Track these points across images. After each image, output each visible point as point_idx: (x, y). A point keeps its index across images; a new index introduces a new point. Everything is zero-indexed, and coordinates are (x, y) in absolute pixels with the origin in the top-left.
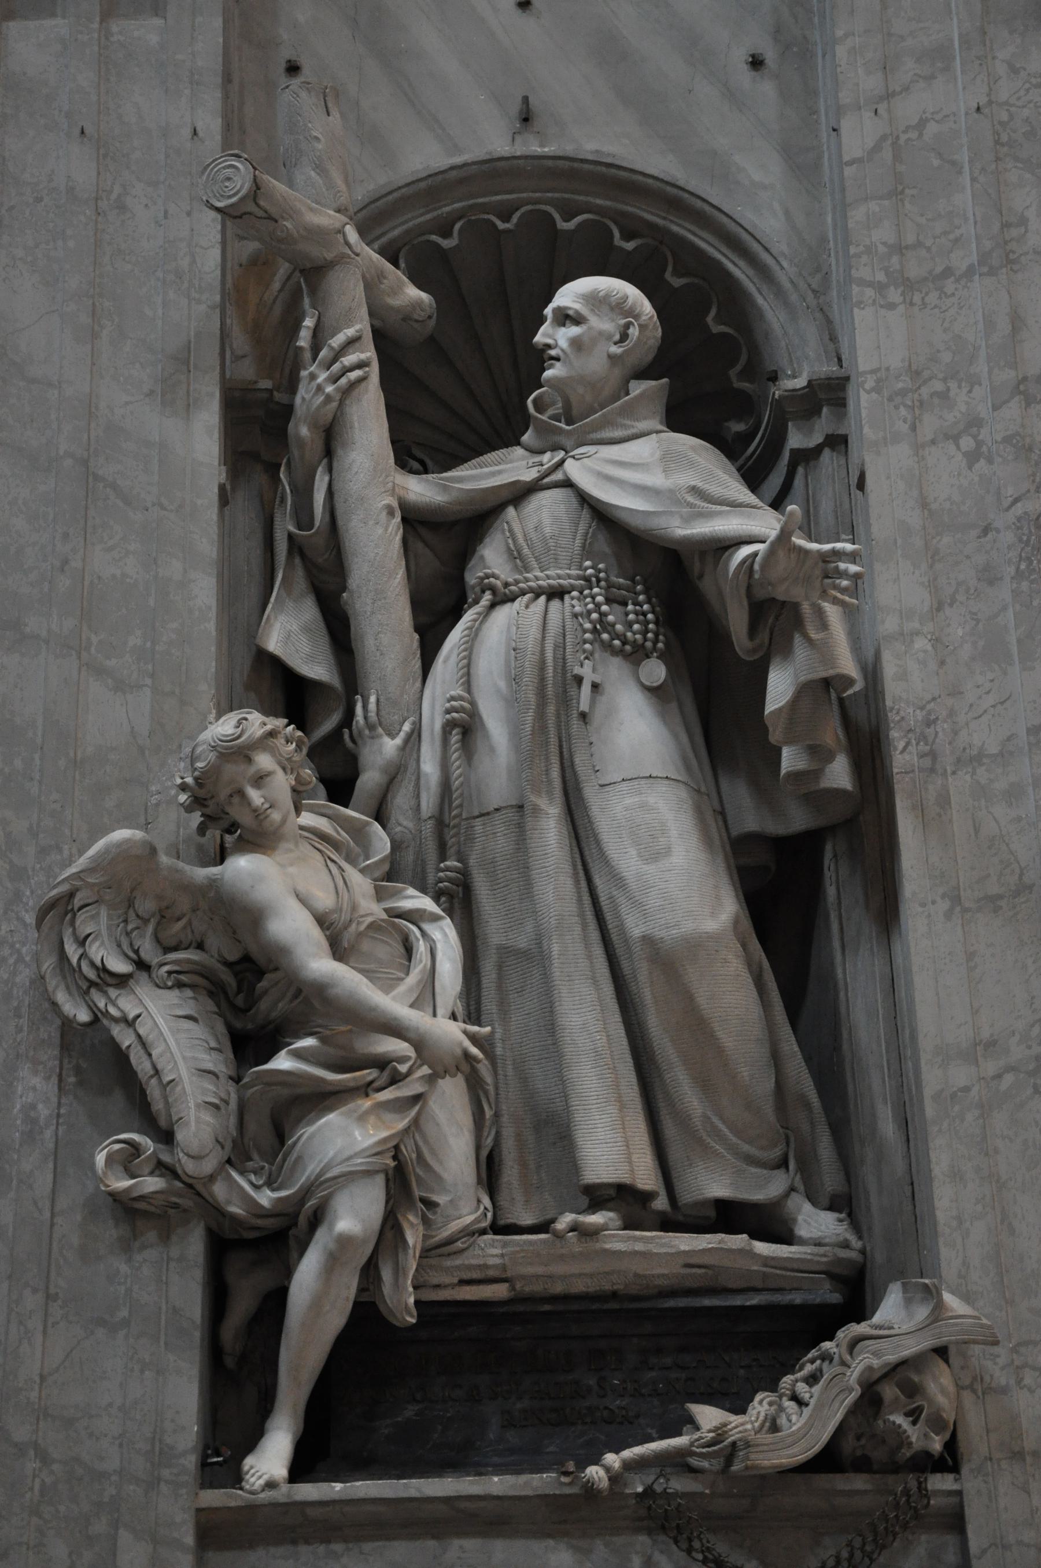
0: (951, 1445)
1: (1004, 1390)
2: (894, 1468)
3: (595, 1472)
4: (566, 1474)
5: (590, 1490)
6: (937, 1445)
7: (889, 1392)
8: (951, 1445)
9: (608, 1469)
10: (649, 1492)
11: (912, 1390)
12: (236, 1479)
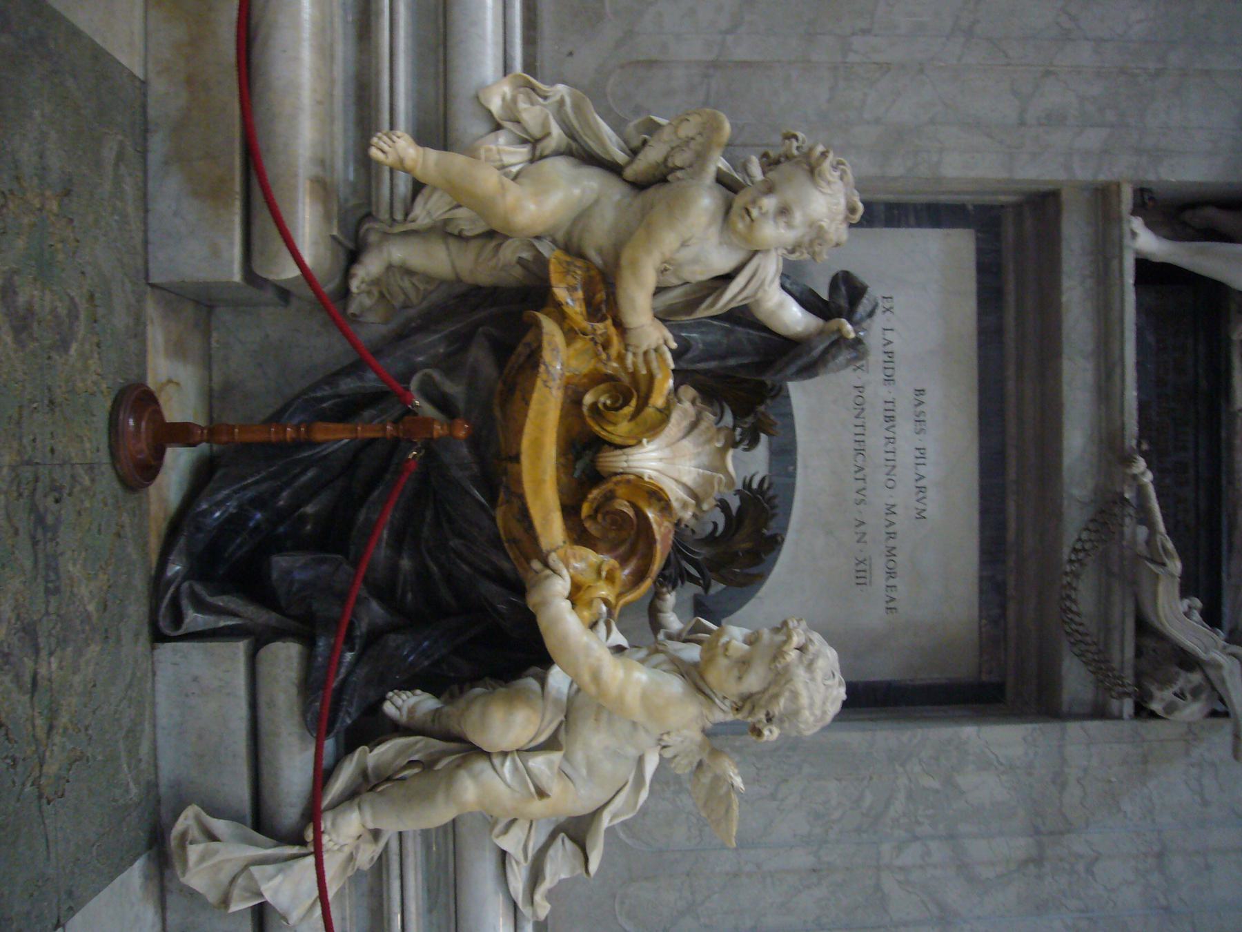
0: (1153, 715)
1: (1187, 753)
2: (1139, 675)
3: (1141, 464)
4: (1139, 444)
5: (1128, 461)
6: (1156, 706)
7: (1196, 678)
8: (1153, 715)
9: (1143, 474)
10: (1124, 501)
11: (1196, 693)
12: (1134, 213)
